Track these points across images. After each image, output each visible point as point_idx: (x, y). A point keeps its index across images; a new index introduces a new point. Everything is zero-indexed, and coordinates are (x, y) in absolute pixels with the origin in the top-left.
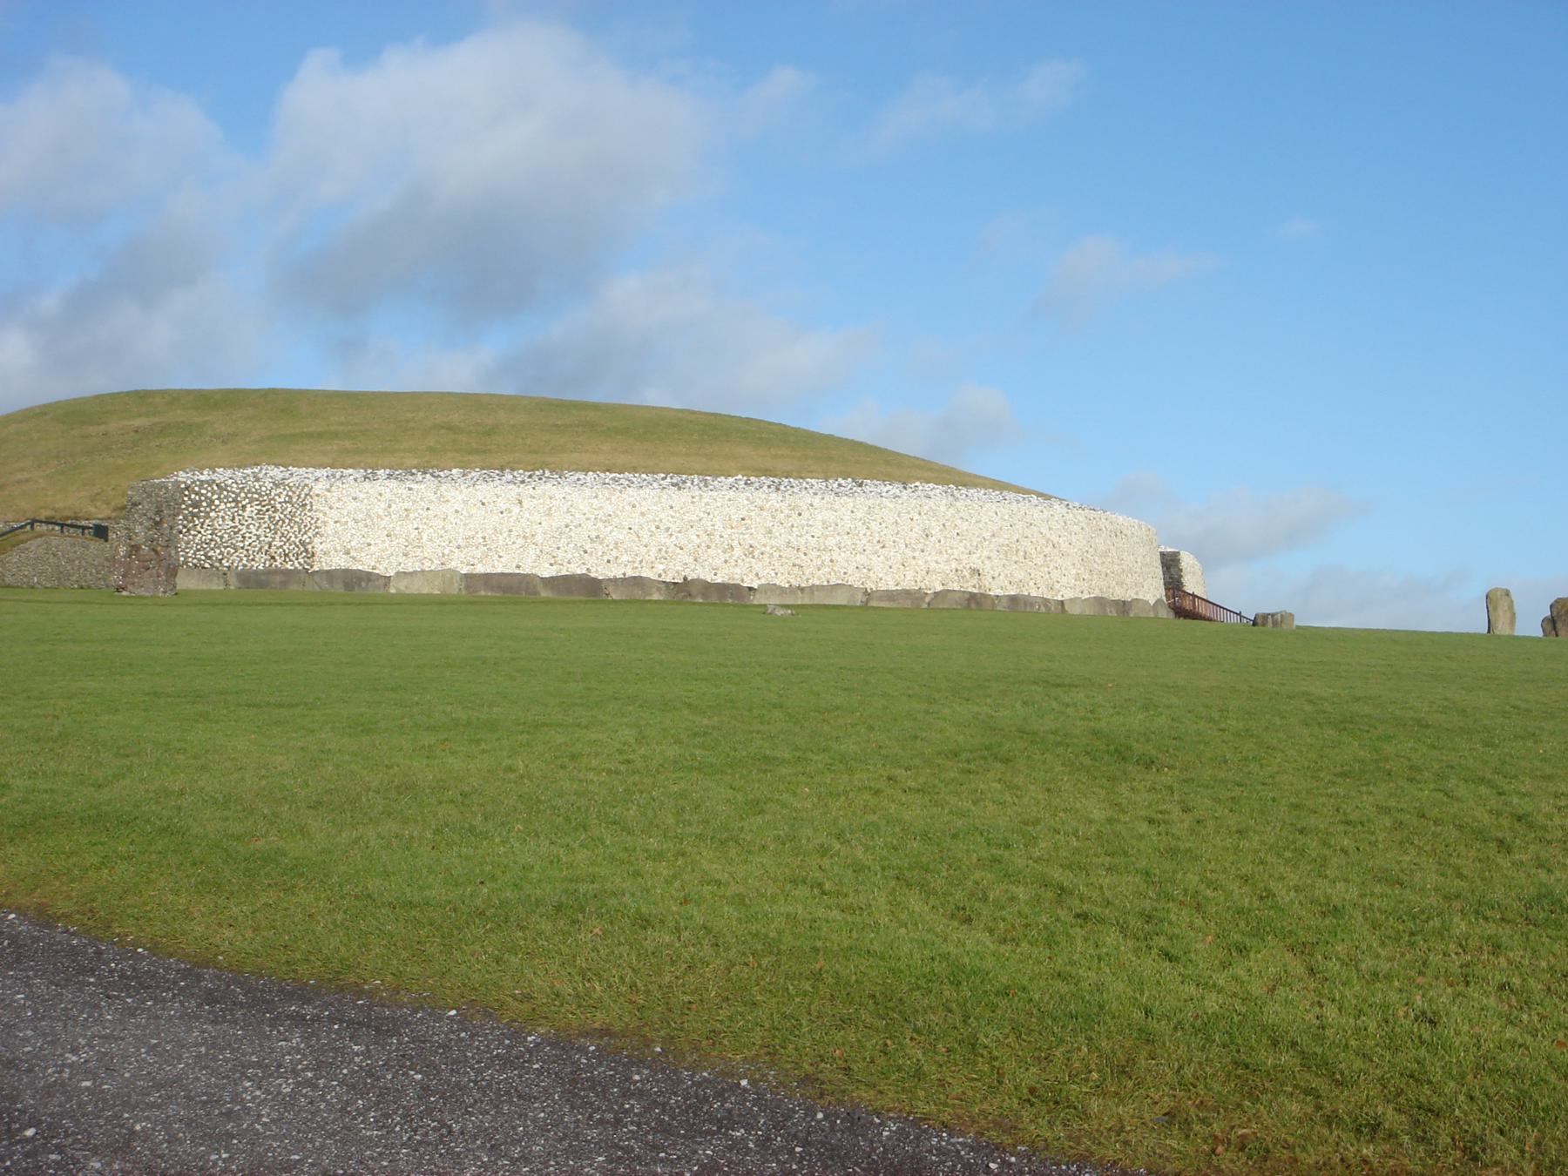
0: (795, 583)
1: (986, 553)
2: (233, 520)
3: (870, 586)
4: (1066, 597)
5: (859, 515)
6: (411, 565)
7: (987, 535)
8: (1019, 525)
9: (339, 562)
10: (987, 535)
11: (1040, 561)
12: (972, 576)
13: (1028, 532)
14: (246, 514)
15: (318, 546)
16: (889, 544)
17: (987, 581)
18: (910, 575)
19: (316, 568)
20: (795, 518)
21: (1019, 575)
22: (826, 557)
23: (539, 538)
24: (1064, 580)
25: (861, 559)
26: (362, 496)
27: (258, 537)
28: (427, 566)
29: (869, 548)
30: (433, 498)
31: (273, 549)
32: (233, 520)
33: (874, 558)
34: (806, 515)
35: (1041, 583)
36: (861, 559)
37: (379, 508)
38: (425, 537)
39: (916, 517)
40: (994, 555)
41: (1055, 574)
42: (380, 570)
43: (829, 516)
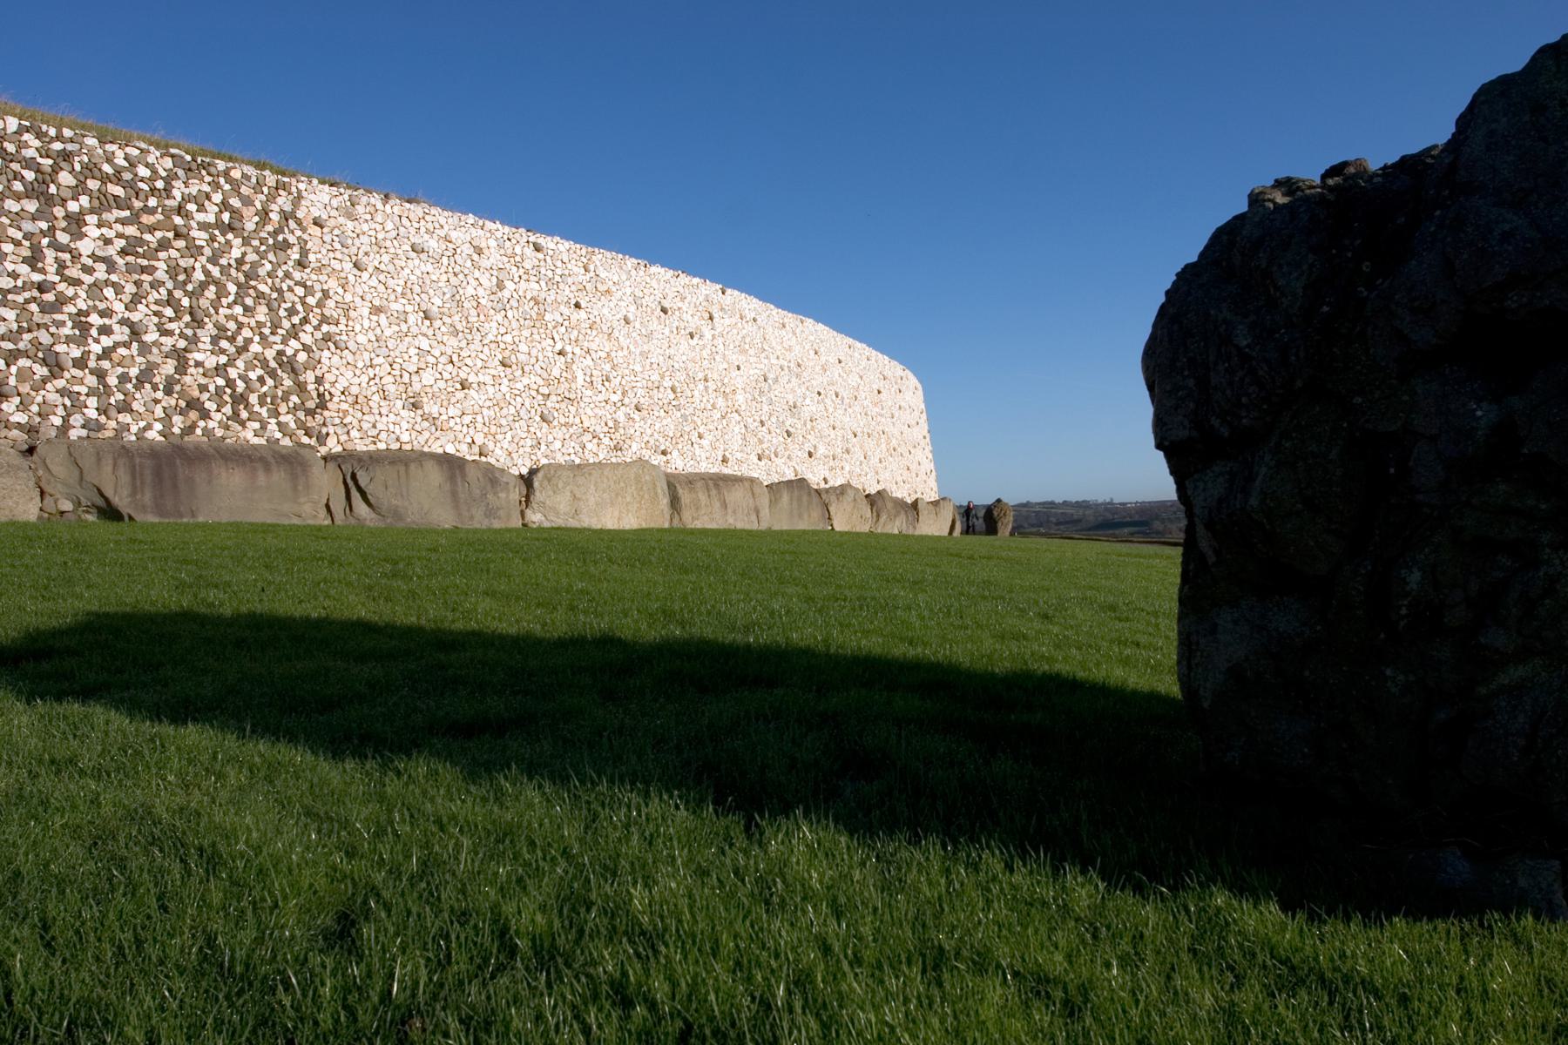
2: (34, 261)
6: (558, 449)
9: (397, 430)
14: (85, 247)
15: (338, 372)
19: (332, 445)
23: (740, 398)
26: (432, 244)
27: (136, 332)
28: (597, 452)
30: (582, 277)
31: (192, 378)
32: (34, 261)
37: (478, 286)
38: (580, 375)
42: (498, 457)
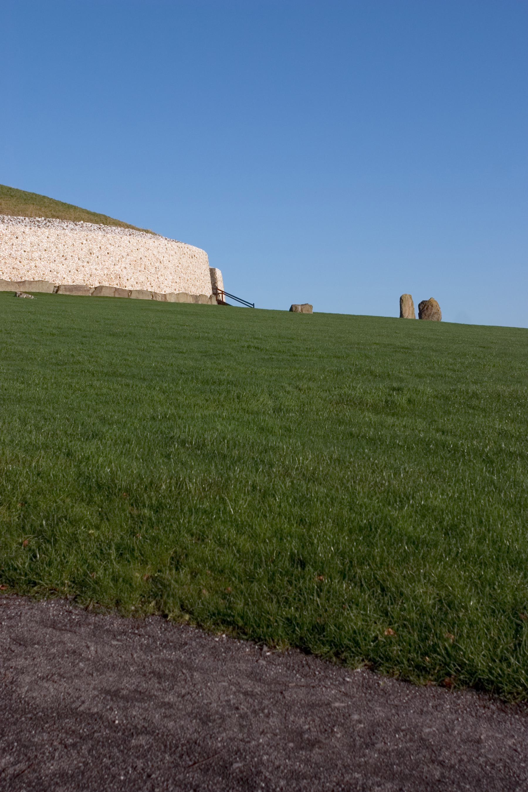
0: (14, 279)
1: (123, 265)
3: (58, 283)
4: (167, 292)
5: (52, 239)
7: (125, 254)
8: (142, 250)
10: (125, 254)
11: (153, 271)
12: (116, 278)
13: (147, 254)
16: (69, 257)
17: (124, 282)
18: (81, 277)
20: (15, 241)
21: (142, 279)
22: (33, 264)
24: (166, 282)
25: (53, 266)
29: (57, 259)
33: (61, 265)
34: (21, 238)
35: (153, 284)
36: (53, 266)
39: (85, 242)
40: (127, 266)
41: (161, 279)
43: (34, 239)
